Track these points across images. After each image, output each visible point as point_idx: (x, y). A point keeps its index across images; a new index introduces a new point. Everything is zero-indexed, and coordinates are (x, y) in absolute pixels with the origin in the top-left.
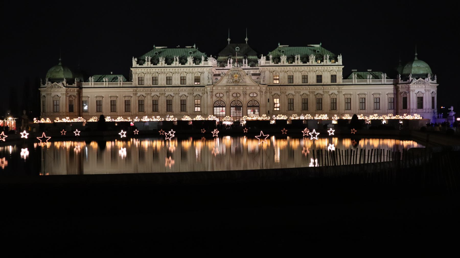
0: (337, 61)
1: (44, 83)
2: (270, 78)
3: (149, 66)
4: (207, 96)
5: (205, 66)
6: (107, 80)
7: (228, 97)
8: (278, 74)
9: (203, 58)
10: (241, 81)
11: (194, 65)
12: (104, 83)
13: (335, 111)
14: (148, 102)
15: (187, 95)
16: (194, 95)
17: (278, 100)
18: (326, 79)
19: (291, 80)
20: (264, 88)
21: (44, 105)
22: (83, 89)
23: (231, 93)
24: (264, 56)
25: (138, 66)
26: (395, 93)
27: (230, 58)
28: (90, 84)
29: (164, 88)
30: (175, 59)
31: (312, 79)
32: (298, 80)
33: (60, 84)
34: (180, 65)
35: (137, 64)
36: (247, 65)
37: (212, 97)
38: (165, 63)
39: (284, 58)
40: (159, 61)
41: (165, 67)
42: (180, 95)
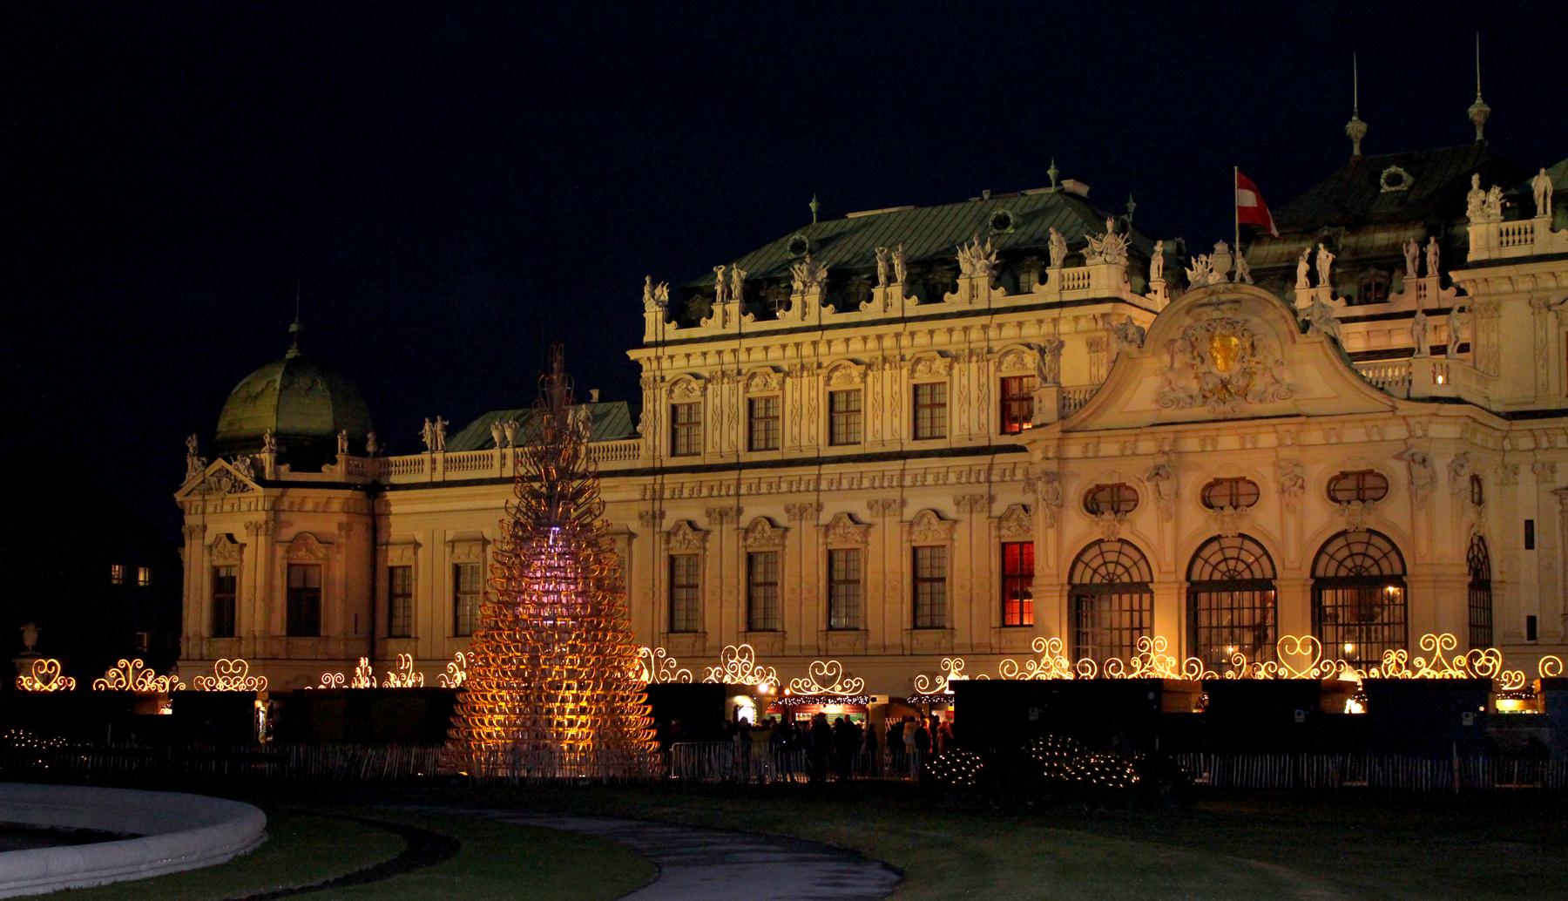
5: (1067, 296)
6: (509, 433)
7: (1170, 513)
9: (1057, 250)
10: (1259, 384)
11: (1000, 298)
12: (496, 452)
14: (801, 572)
15: (950, 511)
22: (391, 495)
24: (1485, 187)
25: (672, 331)
28: (427, 467)
29: (812, 471)
30: (881, 269)
33: (240, 469)
34: (913, 306)
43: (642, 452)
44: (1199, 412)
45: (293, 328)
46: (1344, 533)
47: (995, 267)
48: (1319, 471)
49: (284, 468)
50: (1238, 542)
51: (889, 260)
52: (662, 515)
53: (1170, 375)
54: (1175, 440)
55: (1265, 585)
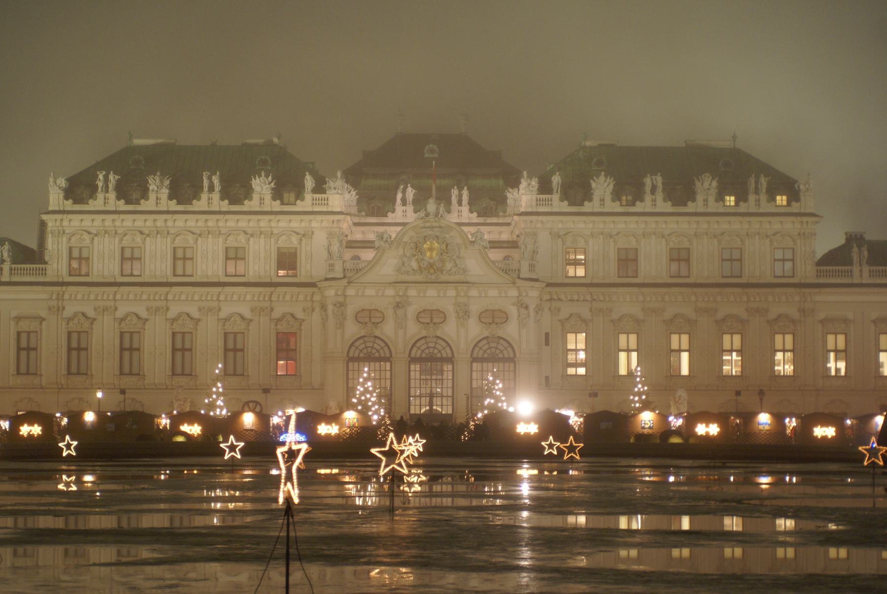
0: (798, 200)
5: (317, 209)
8: (581, 243)
10: (449, 265)
11: (277, 206)
16: (276, 314)
20: (533, 294)
23: (411, 311)
24: (530, 177)
25: (69, 205)
35: (66, 198)
36: (465, 209)
37: (341, 325)
38: (170, 198)
41: (168, 212)
42: (222, 315)
43: (49, 272)
44: (419, 278)
46: (487, 338)
47: (273, 189)
48: (475, 308)
50: (435, 340)
51: (210, 178)
52: (64, 308)
53: (405, 259)
54: (406, 289)
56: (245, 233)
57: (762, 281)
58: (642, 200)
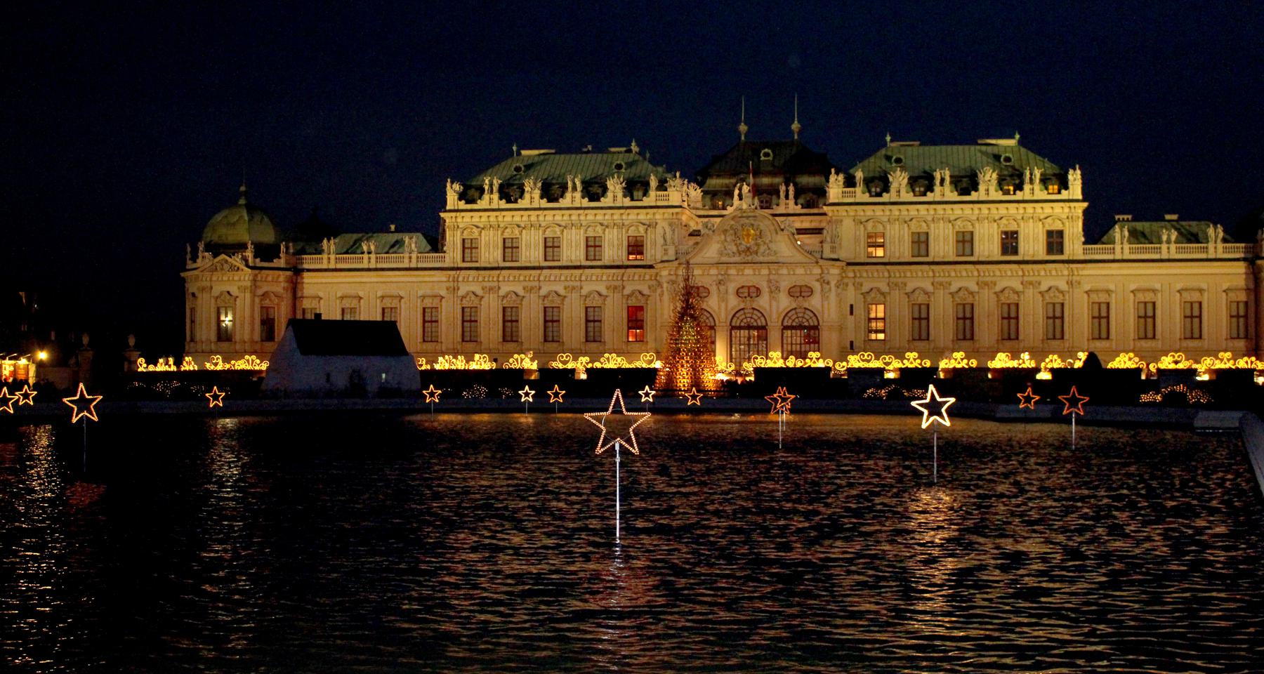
0: (1066, 188)
1: (194, 259)
2: (857, 240)
3: (494, 206)
4: (662, 295)
5: (659, 204)
6: (372, 248)
7: (723, 299)
9: (653, 183)
10: (762, 248)
11: (627, 202)
12: (366, 256)
13: (1057, 342)
15: (604, 292)
16: (627, 292)
17: (881, 308)
18: (1032, 244)
19: (923, 246)
21: (193, 321)
22: (306, 274)
24: (837, 173)
25: (462, 205)
26: (1252, 286)
27: (743, 180)
28: (325, 261)
31: (987, 245)
32: (943, 246)
33: (236, 260)
34: (585, 202)
35: (460, 199)
36: (791, 202)
38: (542, 197)
39: (899, 180)
40: (523, 192)
41: (540, 209)
42: (584, 292)
43: (447, 259)
44: (737, 259)
45: (243, 188)
48: (785, 284)
49: (258, 260)
55: (764, 328)
56: (602, 224)
57: (946, 260)
58: (932, 191)
